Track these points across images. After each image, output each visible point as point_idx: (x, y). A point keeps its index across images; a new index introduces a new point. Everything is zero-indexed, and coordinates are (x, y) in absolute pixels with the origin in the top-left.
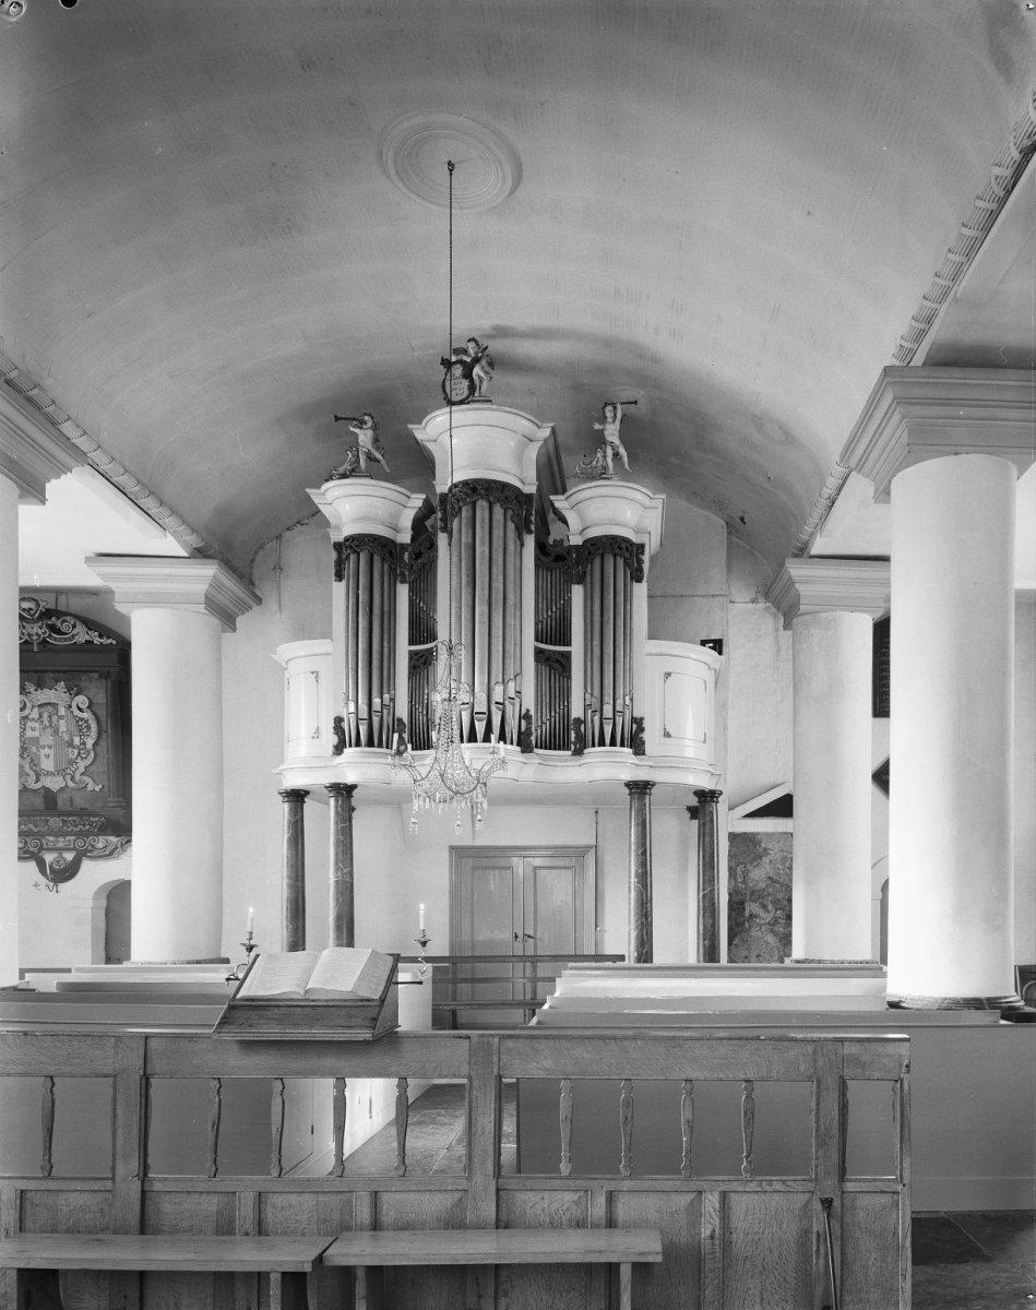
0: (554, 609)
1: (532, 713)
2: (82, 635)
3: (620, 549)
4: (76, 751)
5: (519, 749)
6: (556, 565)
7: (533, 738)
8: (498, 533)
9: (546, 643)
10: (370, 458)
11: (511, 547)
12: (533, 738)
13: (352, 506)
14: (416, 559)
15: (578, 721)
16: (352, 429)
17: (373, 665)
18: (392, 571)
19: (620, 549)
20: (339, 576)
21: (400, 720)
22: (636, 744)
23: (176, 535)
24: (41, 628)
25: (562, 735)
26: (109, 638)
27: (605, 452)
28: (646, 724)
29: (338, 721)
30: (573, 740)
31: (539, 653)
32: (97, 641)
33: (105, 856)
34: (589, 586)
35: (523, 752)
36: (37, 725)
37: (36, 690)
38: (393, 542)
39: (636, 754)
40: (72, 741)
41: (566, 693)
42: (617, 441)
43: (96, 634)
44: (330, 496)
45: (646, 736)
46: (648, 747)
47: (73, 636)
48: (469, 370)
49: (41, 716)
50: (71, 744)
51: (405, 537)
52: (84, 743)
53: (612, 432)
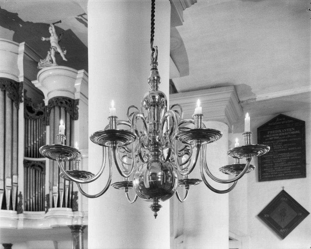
0: (37, 140)
1: (23, 194)
5: (16, 212)
6: (37, 117)
7: (23, 206)
9: (33, 157)
11: (8, 110)
12: (23, 206)
15: (48, 195)
19: (61, 103)
25: (40, 205)
31: (26, 163)
41: (42, 182)
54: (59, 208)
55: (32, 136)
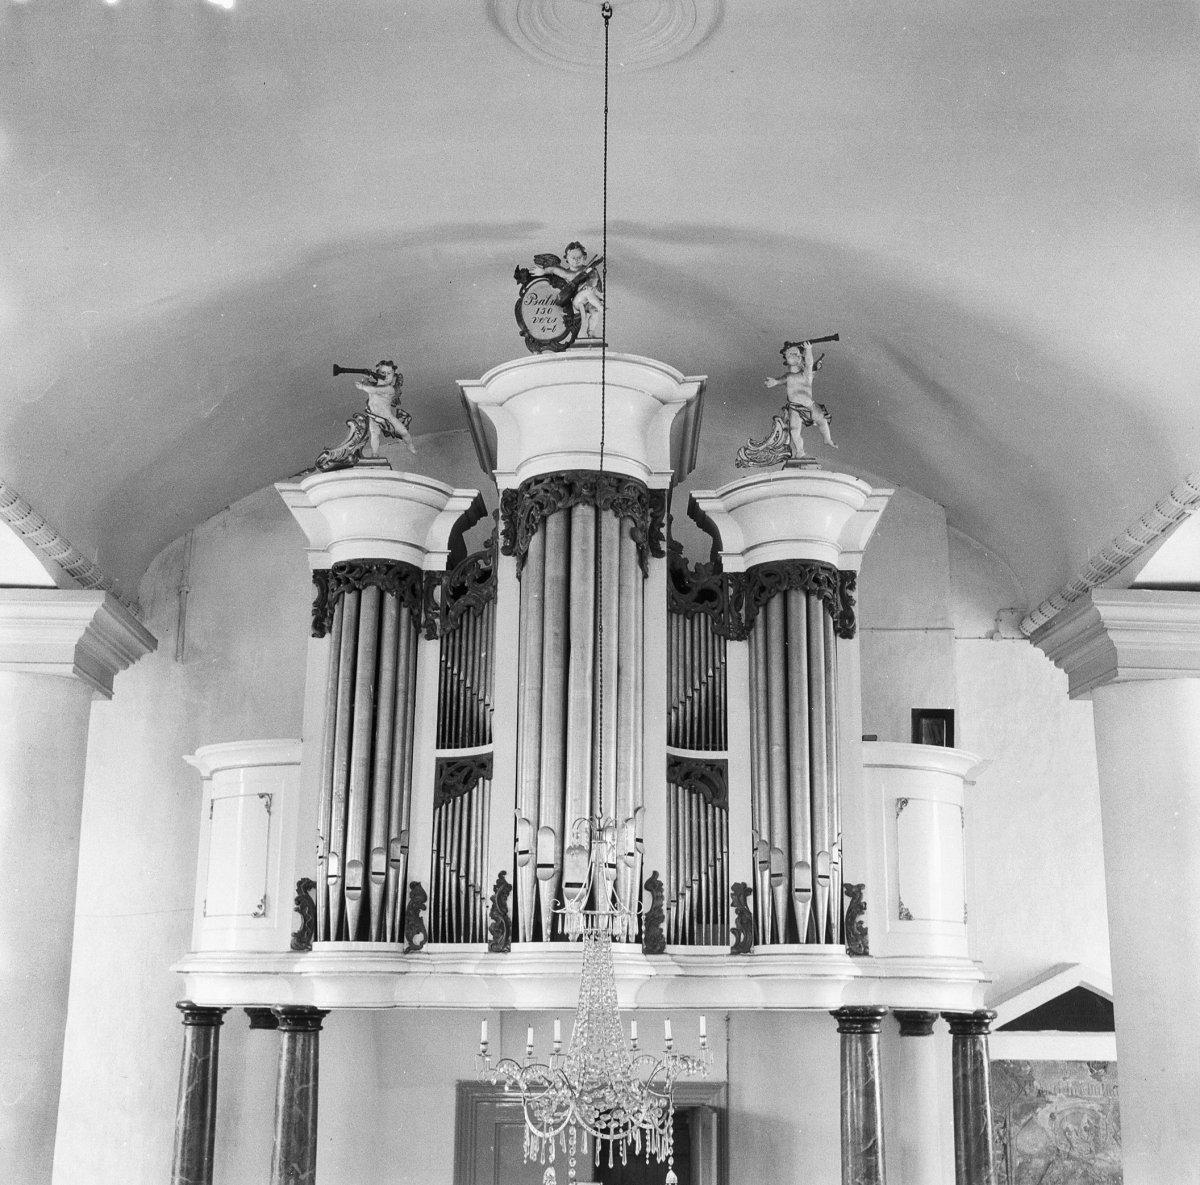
1: (663, 878)
3: (816, 580)
8: (610, 559)
10: (387, 432)
13: (360, 513)
14: (455, 597)
15: (742, 890)
16: (360, 387)
17: (375, 781)
18: (414, 619)
19: (816, 580)
20: (320, 628)
21: (416, 886)
22: (853, 937)
23: (44, 555)
27: (788, 422)
28: (867, 897)
29: (306, 886)
30: (733, 925)
34: (760, 645)
35: (646, 952)
38: (418, 571)
39: (851, 953)
42: (809, 403)
44: (313, 497)
45: (868, 919)
46: (873, 940)
48: (560, 297)
51: (437, 562)
53: (800, 388)
54: (813, 948)
55: (681, 669)
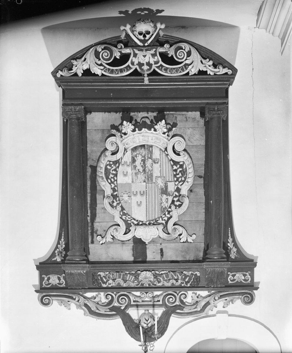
2: (196, 64)
4: (170, 199)
24: (154, 55)
26: (224, 67)
32: (211, 71)
33: (196, 312)
36: (129, 170)
37: (134, 131)
40: (166, 187)
43: (211, 63)
47: (187, 65)
49: (134, 161)
50: (165, 191)
52: (178, 190)
